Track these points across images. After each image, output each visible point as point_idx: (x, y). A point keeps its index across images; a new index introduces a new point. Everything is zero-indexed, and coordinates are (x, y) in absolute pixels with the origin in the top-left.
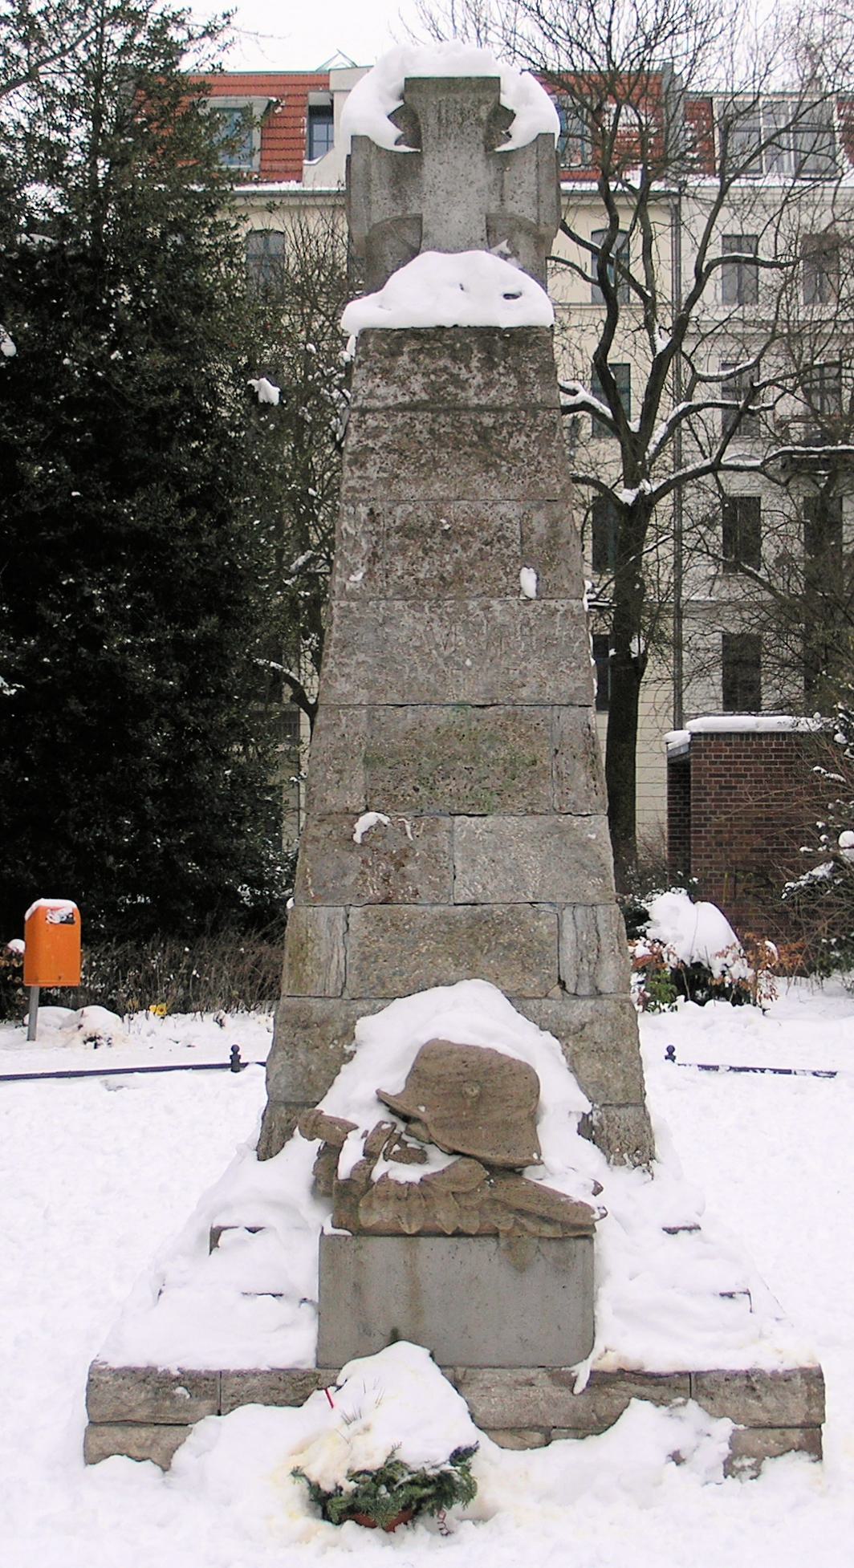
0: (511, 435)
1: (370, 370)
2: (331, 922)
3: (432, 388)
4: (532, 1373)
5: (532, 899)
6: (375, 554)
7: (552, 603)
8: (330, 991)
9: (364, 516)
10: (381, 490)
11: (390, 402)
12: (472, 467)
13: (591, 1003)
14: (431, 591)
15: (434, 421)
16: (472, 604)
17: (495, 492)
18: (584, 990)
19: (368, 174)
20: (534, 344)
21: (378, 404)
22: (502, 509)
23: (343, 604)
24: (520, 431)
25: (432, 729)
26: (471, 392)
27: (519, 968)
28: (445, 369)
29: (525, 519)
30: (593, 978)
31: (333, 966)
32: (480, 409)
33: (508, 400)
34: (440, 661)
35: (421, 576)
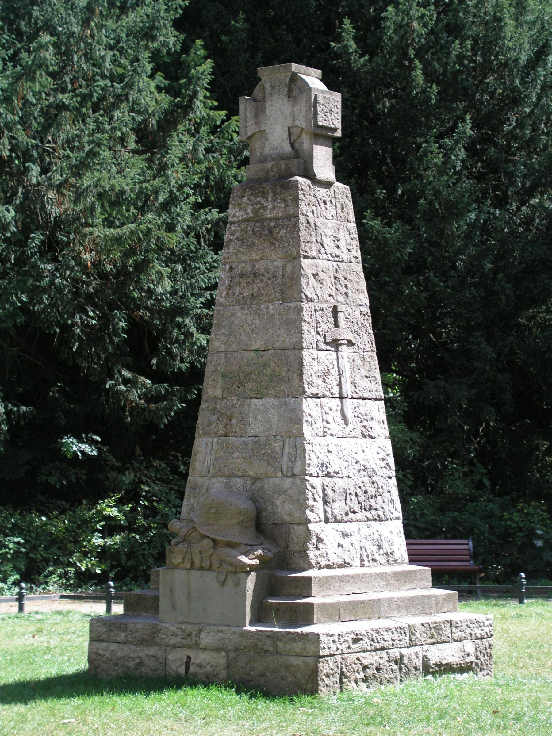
0: (280, 229)
1: (234, 205)
2: (207, 444)
3: (255, 211)
4: (224, 628)
5: (274, 434)
6: (230, 286)
7: (290, 304)
8: (204, 474)
9: (227, 269)
10: (234, 258)
11: (240, 218)
12: (265, 245)
13: (291, 479)
14: (248, 301)
15: (255, 225)
16: (262, 306)
17: (274, 256)
18: (289, 474)
19: (246, 114)
20: (291, 188)
21: (236, 220)
22: (276, 263)
23: (218, 308)
24: (283, 228)
25: (246, 361)
26: (268, 212)
27: (266, 464)
28: (259, 202)
29: (284, 267)
30: (292, 468)
31: (206, 463)
32: (271, 219)
33: (281, 214)
34: (250, 332)
35: (245, 295)
